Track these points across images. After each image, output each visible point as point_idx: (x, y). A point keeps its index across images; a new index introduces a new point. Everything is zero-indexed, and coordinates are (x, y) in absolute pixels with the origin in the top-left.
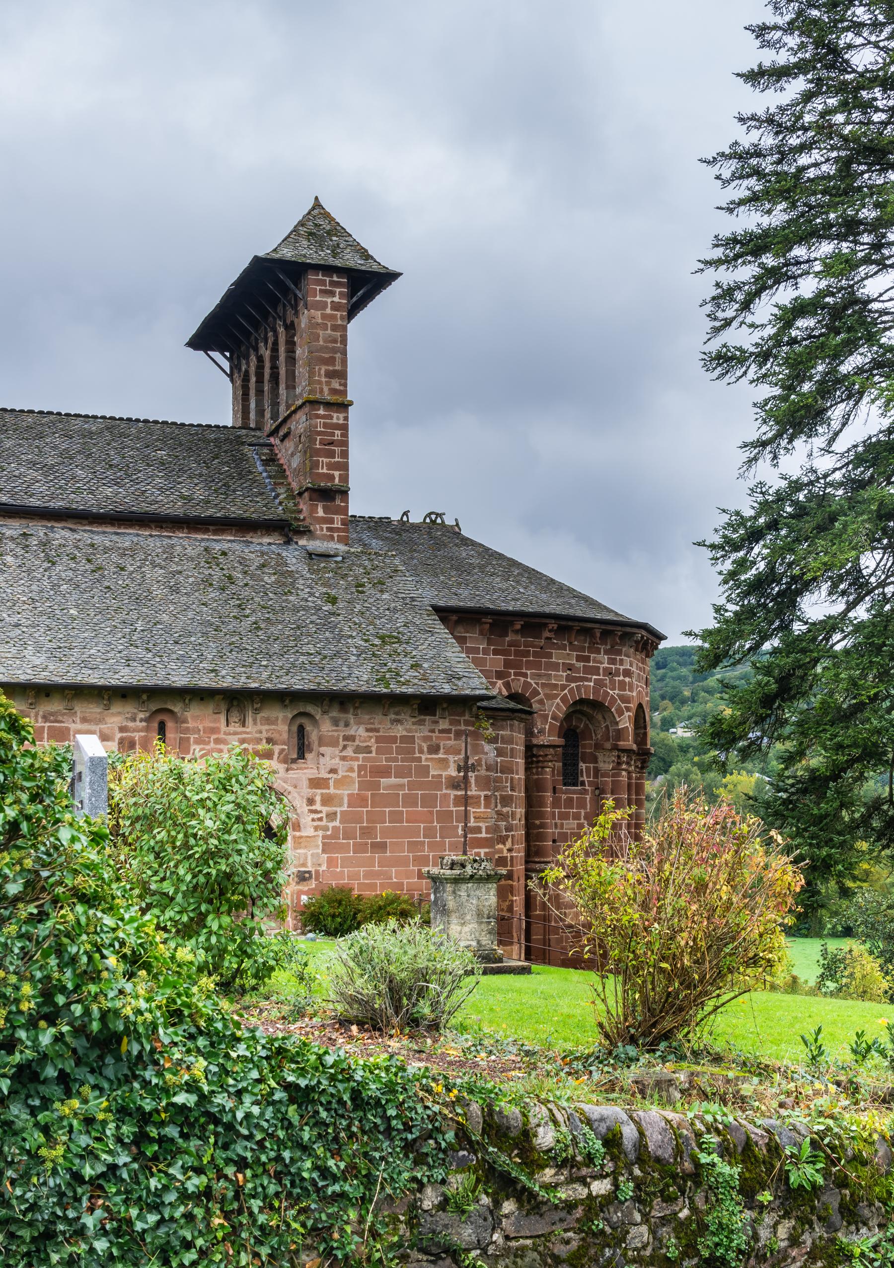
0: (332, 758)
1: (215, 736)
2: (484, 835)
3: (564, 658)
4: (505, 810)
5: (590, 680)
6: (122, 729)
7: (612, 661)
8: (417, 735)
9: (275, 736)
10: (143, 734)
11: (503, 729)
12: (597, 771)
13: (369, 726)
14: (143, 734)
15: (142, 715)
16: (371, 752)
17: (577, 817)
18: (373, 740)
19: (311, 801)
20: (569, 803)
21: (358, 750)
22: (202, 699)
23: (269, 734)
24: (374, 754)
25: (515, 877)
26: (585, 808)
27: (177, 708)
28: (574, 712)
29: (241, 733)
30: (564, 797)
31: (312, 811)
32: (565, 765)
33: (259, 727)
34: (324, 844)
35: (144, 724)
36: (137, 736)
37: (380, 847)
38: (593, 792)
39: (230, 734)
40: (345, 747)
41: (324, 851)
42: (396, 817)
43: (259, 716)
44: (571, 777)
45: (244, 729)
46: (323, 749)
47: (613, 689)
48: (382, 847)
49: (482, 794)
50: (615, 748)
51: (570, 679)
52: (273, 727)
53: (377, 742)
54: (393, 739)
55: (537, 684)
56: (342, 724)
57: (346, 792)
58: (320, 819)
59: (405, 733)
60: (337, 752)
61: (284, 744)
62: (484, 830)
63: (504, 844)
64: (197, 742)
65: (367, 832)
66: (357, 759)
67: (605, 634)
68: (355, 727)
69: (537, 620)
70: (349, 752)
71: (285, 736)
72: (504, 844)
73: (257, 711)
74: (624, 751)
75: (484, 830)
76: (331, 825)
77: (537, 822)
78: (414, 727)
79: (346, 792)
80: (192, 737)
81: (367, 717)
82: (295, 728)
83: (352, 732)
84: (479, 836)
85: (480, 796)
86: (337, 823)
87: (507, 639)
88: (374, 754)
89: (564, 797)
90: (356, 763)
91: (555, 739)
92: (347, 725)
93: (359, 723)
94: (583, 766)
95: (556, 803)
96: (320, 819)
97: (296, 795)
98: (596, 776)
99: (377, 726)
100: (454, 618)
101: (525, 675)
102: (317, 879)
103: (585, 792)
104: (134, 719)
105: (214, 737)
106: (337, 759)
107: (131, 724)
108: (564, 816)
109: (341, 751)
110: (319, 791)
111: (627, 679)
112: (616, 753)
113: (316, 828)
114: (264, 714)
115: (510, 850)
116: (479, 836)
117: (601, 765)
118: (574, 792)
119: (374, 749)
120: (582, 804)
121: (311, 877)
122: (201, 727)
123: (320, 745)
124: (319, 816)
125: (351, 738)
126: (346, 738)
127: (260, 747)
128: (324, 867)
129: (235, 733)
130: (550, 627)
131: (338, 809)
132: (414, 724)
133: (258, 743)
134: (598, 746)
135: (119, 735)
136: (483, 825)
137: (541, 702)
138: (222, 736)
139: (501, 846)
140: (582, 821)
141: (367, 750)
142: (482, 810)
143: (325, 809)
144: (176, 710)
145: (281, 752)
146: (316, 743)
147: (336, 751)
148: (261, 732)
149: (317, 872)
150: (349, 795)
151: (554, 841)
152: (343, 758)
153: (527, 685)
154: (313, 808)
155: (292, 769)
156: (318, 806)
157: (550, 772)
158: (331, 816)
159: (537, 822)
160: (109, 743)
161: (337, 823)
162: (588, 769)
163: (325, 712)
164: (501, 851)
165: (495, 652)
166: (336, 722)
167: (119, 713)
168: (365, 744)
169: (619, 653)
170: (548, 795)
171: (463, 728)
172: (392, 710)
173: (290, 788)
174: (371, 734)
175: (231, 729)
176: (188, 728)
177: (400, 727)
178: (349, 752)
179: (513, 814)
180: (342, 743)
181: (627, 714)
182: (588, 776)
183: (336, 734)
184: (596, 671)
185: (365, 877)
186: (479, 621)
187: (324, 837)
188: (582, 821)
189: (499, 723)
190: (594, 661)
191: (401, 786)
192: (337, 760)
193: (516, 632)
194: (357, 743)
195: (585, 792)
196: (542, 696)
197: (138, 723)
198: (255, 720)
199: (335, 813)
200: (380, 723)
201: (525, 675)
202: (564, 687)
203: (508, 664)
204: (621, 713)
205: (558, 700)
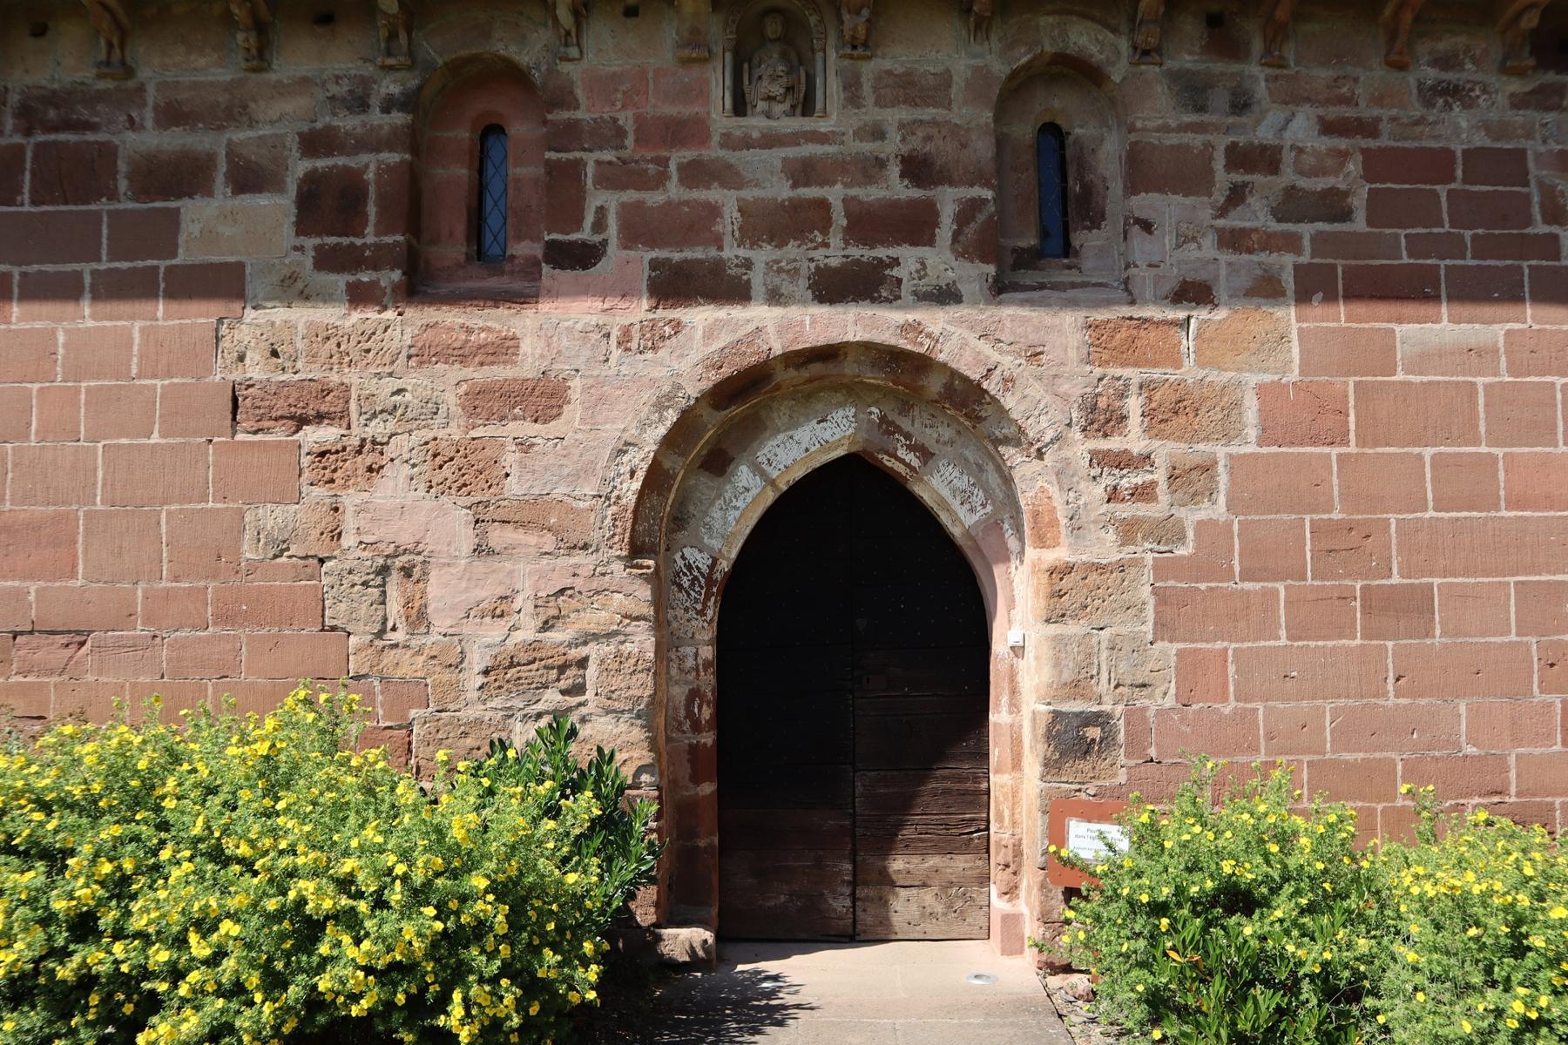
0: (1183, 240)
1: (688, 154)
6: (313, 143)
8: (1533, 147)
9: (942, 150)
10: (393, 158)
13: (1334, 112)
14: (393, 158)
15: (390, 86)
16: (1345, 215)
18: (1353, 167)
19: (1101, 417)
21: (1292, 206)
22: (631, 12)
23: (915, 143)
24: (1359, 224)
27: (529, 49)
29: (794, 139)
31: (1102, 459)
33: (871, 113)
34: (1160, 595)
35: (399, 118)
36: (370, 165)
37: (1403, 610)
39: (747, 143)
40: (1237, 196)
41: (1164, 629)
42: (1467, 485)
43: (869, 70)
45: (807, 124)
46: (1146, 203)
48: (1411, 609)
52: (929, 113)
53: (1369, 175)
54: (1438, 164)
56: (1220, 99)
57: (1252, 379)
58: (1144, 493)
59: (1481, 140)
60: (1205, 214)
61: (979, 179)
64: (612, 178)
65: (1345, 545)
66: (1291, 243)
68: (1274, 116)
70: (1256, 215)
71: (983, 148)
73: (861, 46)
76: (1190, 517)
78: (1519, 117)
79: (1252, 379)
80: (591, 159)
81: (1324, 74)
82: (1024, 131)
83: (1264, 133)
86: (1217, 509)
88: (1359, 224)
90: (1288, 260)
92: (1241, 104)
93: (1293, 98)
96: (1144, 493)
97: (1036, 391)
99: (1366, 111)
102: (1135, 746)
104: (359, 103)
105: (678, 157)
106: (1208, 242)
107: (348, 123)
109: (1222, 212)
110: (1134, 375)
113: (1128, 531)
114: (895, 58)
119: (1359, 202)
121: (1108, 740)
122: (626, 119)
123: (1132, 188)
124: (1139, 479)
125: (1265, 159)
126: (1240, 158)
127: (872, 194)
128: (1164, 698)
129: (771, 141)
131: (1221, 452)
132: (1518, 102)
133: (869, 179)
135: (301, 167)
138: (714, 152)
141: (1333, 206)
143: (1165, 451)
144: (525, 58)
145: (968, 211)
146: (1116, 187)
147: (1202, 209)
148: (878, 134)
149: (1135, 717)
150: (1261, 390)
152: (1233, 240)
154: (1114, 444)
155: (1016, 287)
156: (1133, 439)
158: (1191, 479)
160: (263, 201)
161: (1217, 509)
163: (1144, 53)
166: (1193, 92)
167: (305, 81)
168: (1320, 184)
172: (1423, 49)
173: (1007, 362)
174: (1343, 143)
175: (755, 124)
176: (573, 125)
177: (1461, 118)
178: (1256, 215)
180: (1223, 178)
183: (1196, 140)
185: (1343, 737)
187: (1160, 569)
191: (1481, 355)
192: (1209, 247)
194: (1288, 176)
197: (376, 117)
198: (852, 89)
199: (1207, 468)
200: (1378, 101)
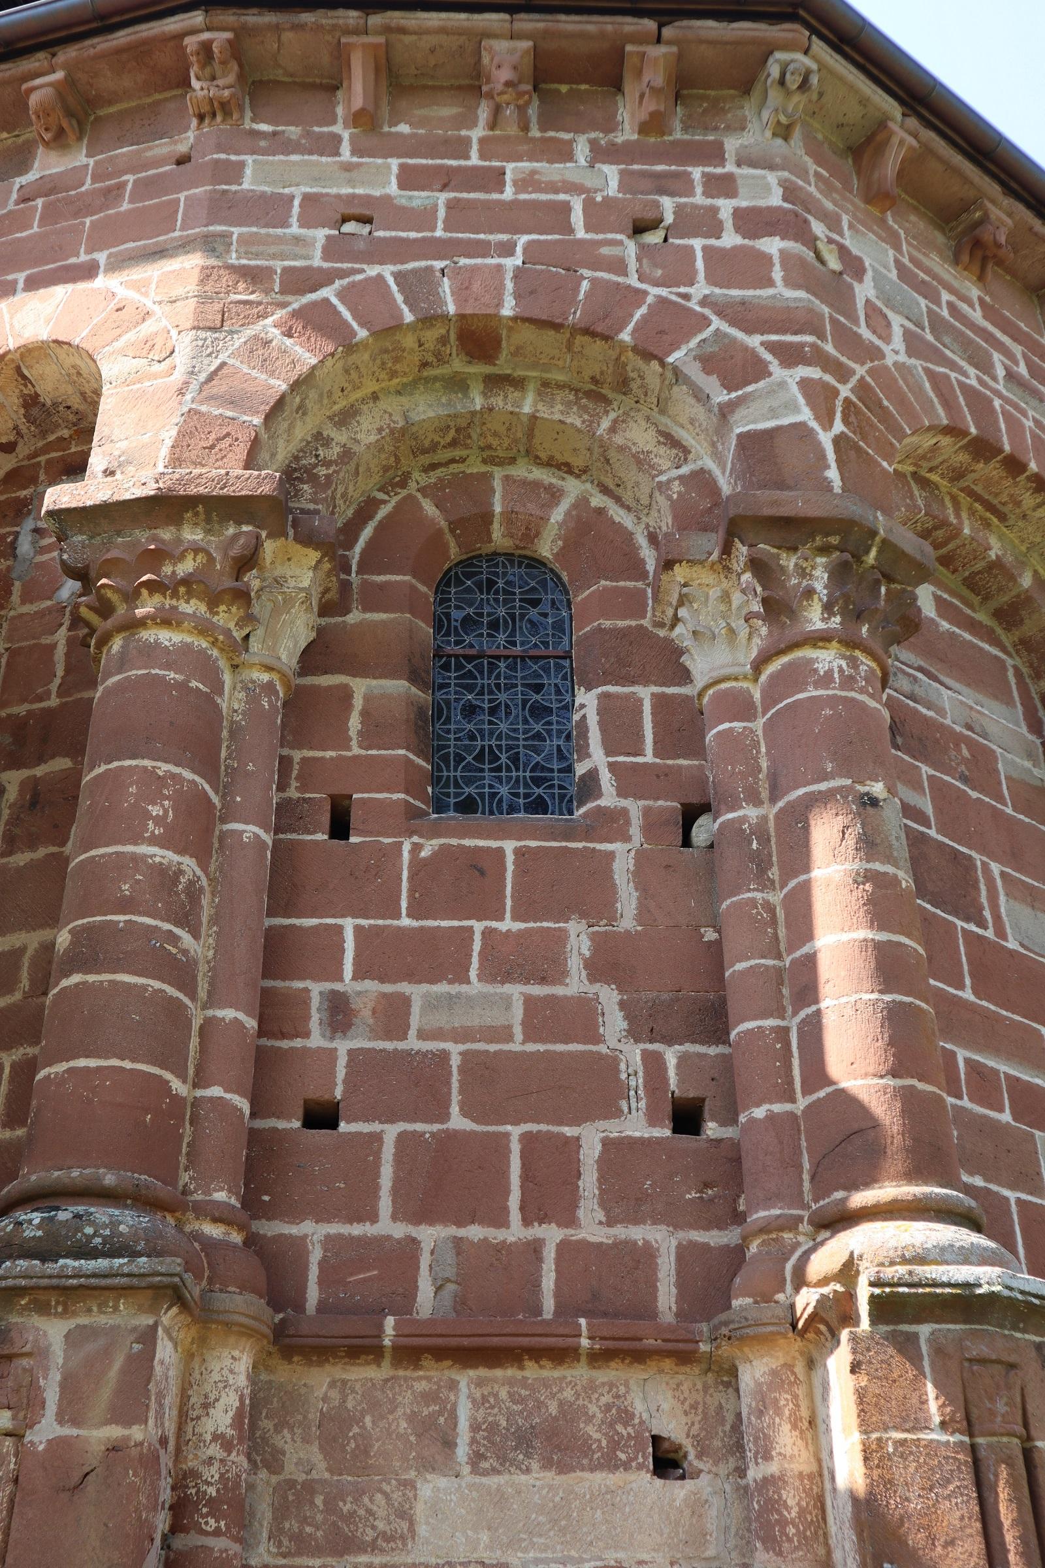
5: (507, 250)
17: (533, 961)
20: (472, 883)
30: (413, 849)
55: (138, 286)
108: (439, 959)
188: (576, 984)
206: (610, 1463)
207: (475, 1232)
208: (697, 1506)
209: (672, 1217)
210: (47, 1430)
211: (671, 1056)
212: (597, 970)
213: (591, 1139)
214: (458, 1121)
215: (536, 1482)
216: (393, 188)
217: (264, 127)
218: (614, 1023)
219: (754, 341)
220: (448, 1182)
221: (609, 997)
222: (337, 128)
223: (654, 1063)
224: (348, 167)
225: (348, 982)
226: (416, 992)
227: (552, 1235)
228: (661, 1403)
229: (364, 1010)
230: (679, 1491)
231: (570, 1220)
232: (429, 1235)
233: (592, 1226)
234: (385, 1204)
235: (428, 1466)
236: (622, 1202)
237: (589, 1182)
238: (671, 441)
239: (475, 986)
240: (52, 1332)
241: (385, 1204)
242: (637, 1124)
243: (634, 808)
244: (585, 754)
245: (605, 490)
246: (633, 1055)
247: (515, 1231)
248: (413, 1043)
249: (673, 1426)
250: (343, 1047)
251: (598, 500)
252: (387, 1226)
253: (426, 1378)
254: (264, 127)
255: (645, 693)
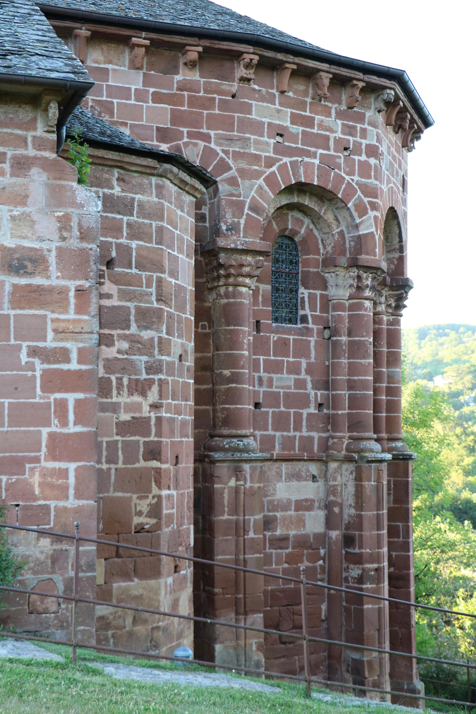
2: (74, 366)
3: (271, 116)
4: (146, 334)
5: (314, 155)
7: (350, 131)
11: (141, 189)
12: (326, 300)
17: (294, 369)
25: (168, 453)
26: (308, 356)
28: (290, 207)
30: (274, 337)
32: (275, 290)
38: (320, 333)
44: (286, 308)
47: (351, 173)
49: (72, 285)
50: (354, 264)
51: (278, 148)
55: (226, 152)
62: (74, 356)
63: (144, 394)
67: (339, 82)
69: (226, 45)
72: (144, 394)
74: (368, 268)
75: (74, 356)
77: (227, 373)
84: (65, 367)
85: (67, 290)
87: (178, 78)
89: (274, 337)
91: (255, 242)
94: (303, 292)
95: (259, 346)
98: (325, 308)
100: (84, 31)
101: (207, 138)
103: (308, 331)
111: (372, 161)
112: (354, 272)
115: (155, 407)
116: (65, 367)
117: (332, 292)
118: (289, 332)
120: (302, 350)
130: (247, 57)
134: (329, 262)
136: (73, 347)
137: (232, 182)
139: (137, 398)
140: (303, 376)
142: (71, 315)
151: (257, 405)
153: (209, 153)
157: (249, 293)
159: (227, 373)
162: (312, 298)
164: (138, 407)
165: (157, 98)
169: (361, 118)
170: (246, 332)
171: (31, 152)
179: (164, 346)
181: (372, 214)
182: (313, 308)
184: (323, 142)
186: (124, 41)
188: (303, 376)
189: (136, 179)
190: (321, 126)
193: (192, 65)
195: (308, 331)
196: (233, 172)
201: (207, 138)
202: (270, 162)
203: (177, 118)
204: (363, 212)
205: (261, 181)
206: (306, 480)
207: (285, 433)
208: (318, 487)
209: (318, 432)
210: (248, 485)
211: (319, 393)
212: (308, 372)
213: (305, 412)
214: (283, 409)
215: (295, 483)
216: (288, 124)
217: (256, 87)
218: (309, 385)
219: (366, 200)
220: (281, 422)
221: (309, 378)
222: (274, 91)
223: (316, 394)
224: (278, 111)
225: (262, 374)
226: (274, 376)
227: (298, 434)
228: (313, 468)
229: (265, 380)
230: (316, 484)
231: (301, 431)
232: (278, 434)
233: (305, 433)
234: (270, 427)
235: (278, 481)
236: (310, 428)
237: (304, 423)
238: (337, 220)
239: (285, 375)
240: (247, 467)
241: (270, 427)
242: (313, 410)
243: (315, 327)
244: (303, 308)
245: (313, 223)
246: (313, 393)
247: (292, 434)
248: (274, 389)
249: (315, 473)
250: (262, 390)
251: (311, 226)
252: (271, 432)
253: (277, 465)
254: (256, 87)
255: (318, 292)
